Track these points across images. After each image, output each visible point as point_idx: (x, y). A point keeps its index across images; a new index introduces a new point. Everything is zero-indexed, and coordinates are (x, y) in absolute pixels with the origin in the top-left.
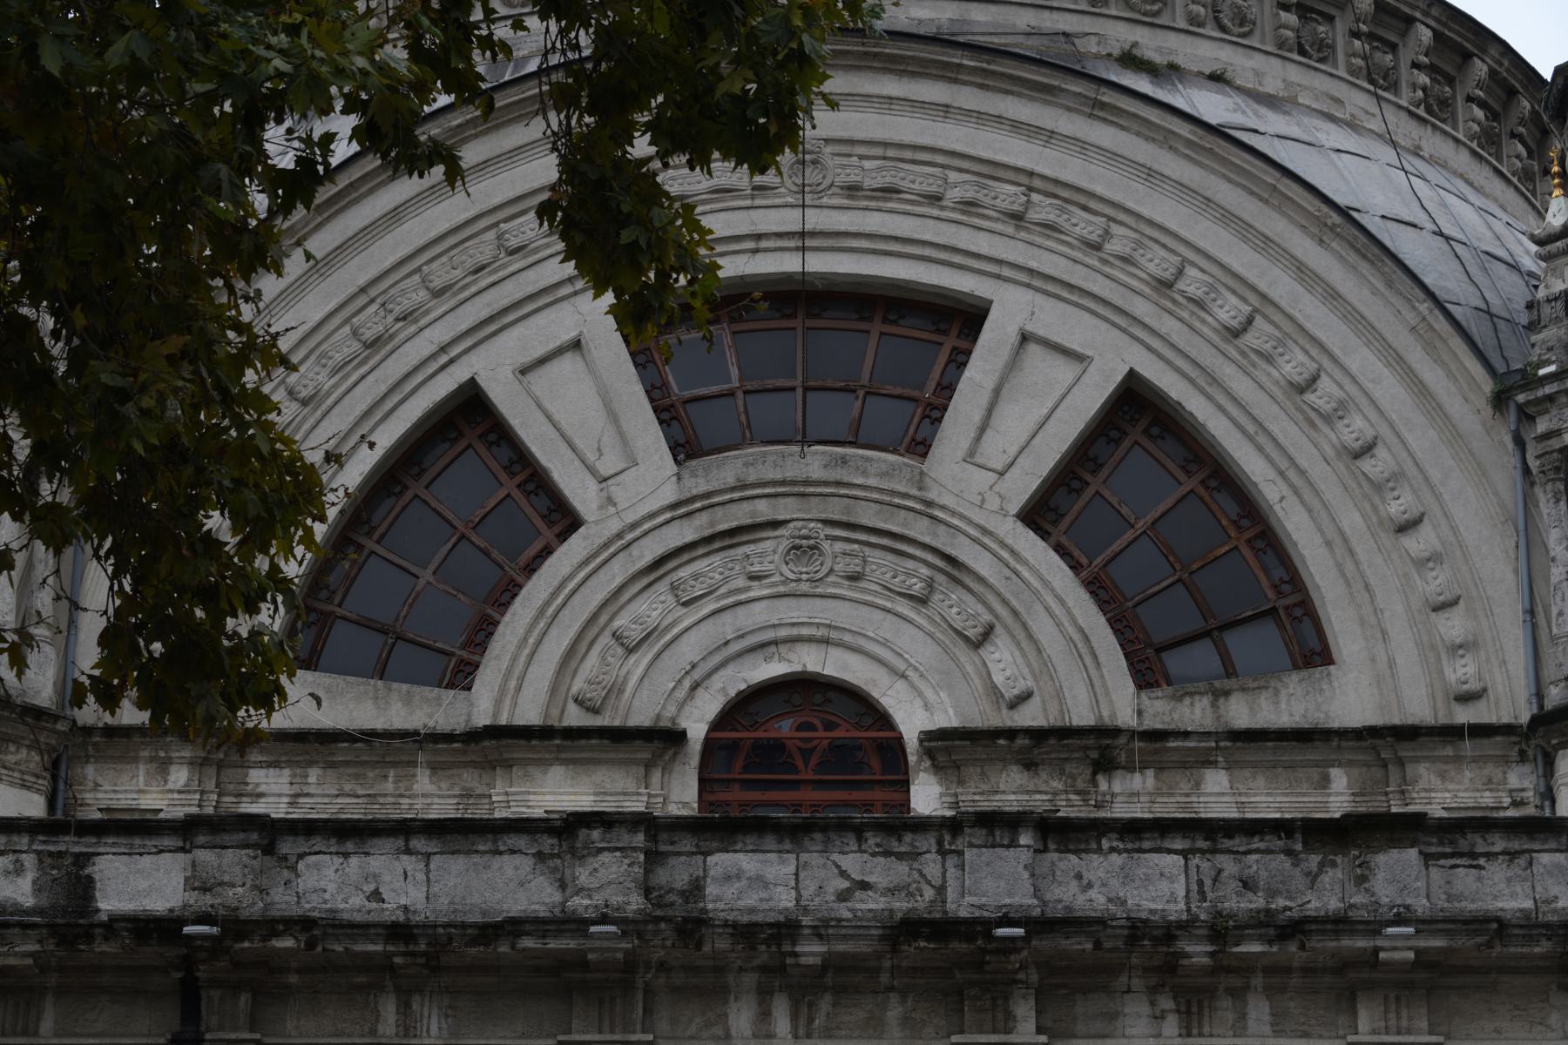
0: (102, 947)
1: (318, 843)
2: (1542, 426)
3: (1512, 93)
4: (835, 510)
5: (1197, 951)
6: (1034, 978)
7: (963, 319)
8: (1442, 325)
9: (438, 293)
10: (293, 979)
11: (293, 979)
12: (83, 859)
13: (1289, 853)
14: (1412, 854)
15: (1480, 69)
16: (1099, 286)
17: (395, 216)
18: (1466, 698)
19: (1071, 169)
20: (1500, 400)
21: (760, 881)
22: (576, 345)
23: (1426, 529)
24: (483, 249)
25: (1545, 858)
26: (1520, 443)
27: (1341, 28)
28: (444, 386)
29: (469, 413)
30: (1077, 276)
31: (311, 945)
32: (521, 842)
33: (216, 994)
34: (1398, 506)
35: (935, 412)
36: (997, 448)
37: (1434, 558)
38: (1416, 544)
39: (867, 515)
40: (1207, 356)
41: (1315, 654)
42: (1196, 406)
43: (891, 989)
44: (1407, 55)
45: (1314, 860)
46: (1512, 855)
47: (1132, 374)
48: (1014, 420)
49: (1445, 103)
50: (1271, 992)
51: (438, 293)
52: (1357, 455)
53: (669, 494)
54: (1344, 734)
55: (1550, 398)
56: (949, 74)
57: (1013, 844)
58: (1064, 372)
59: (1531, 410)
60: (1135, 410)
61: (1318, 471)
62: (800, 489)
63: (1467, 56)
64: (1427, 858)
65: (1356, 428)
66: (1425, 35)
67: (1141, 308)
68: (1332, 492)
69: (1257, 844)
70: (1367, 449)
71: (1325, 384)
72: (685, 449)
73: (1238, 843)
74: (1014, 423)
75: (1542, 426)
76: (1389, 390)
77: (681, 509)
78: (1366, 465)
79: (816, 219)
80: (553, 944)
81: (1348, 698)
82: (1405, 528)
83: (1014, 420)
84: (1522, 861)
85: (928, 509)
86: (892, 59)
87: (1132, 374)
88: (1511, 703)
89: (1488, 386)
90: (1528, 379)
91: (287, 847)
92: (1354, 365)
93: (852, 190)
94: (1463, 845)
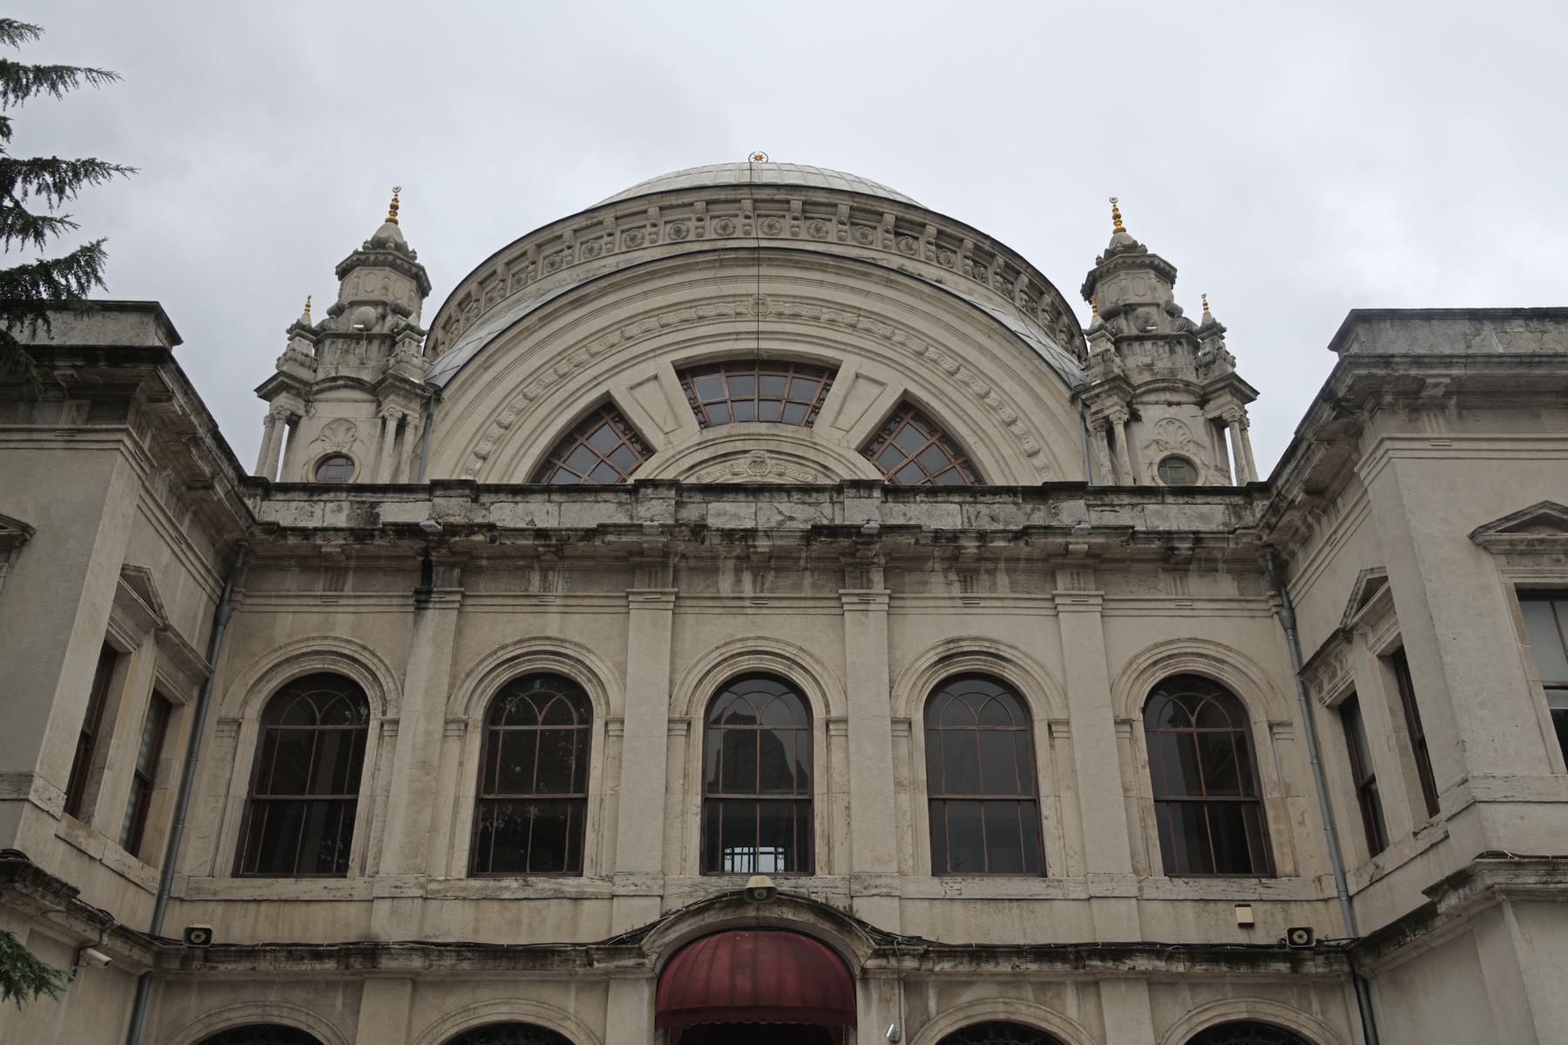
0: (378, 542)
1: (502, 497)
2: (1094, 408)
3: (1060, 314)
4: (773, 446)
5: (970, 546)
6: (883, 561)
7: (826, 371)
8: (1045, 369)
9: (593, 355)
10: (484, 563)
11: (484, 563)
12: (374, 505)
13: (1015, 504)
14: (1082, 502)
15: (1048, 299)
16: (890, 354)
17: (575, 323)
19: (877, 307)
20: (1074, 399)
21: (736, 516)
22: (656, 377)
23: (1041, 455)
24: (615, 337)
25: (1151, 507)
26: (1083, 418)
27: (990, 271)
28: (595, 394)
29: (606, 410)
30: (881, 350)
31: (493, 540)
32: (610, 496)
33: (441, 569)
34: (1029, 446)
35: (816, 410)
36: (844, 422)
37: (1046, 468)
39: (787, 448)
40: (940, 383)
42: (935, 404)
43: (806, 569)
44: (1018, 286)
45: (1029, 507)
46: (1133, 506)
47: (906, 392)
48: (851, 412)
49: (1033, 310)
50: (1008, 571)
51: (593, 355)
52: (1009, 425)
53: (697, 439)
55: (1097, 396)
56: (823, 268)
57: (870, 497)
58: (876, 390)
60: (907, 409)
61: (991, 430)
62: (757, 437)
63: (1042, 293)
64: (1088, 506)
65: (1008, 413)
66: (1026, 280)
67: (909, 363)
68: (998, 440)
69: (998, 499)
70: (1014, 422)
71: (993, 394)
72: (705, 424)
73: (988, 498)
74: (853, 410)
75: (1094, 408)
76: (1022, 397)
77: (702, 445)
78: (1013, 428)
79: (763, 327)
80: (624, 539)
82: (1031, 455)
84: (1139, 508)
85: (814, 446)
86: (797, 262)
87: (906, 392)
89: (1067, 394)
90: (1087, 389)
91: (485, 498)
92: (1006, 387)
93: (780, 315)
94: (1107, 501)
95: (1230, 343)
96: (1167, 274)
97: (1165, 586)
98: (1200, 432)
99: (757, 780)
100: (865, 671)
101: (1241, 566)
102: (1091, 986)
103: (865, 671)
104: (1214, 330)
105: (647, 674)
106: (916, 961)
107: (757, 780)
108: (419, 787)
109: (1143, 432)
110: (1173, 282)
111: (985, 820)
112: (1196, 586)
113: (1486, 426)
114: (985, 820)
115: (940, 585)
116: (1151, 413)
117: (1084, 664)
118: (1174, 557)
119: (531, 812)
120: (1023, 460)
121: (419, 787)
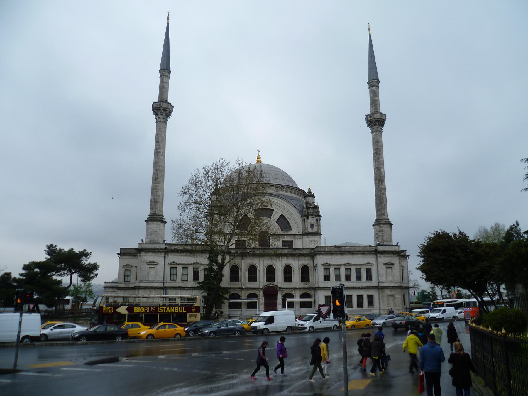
41: (291, 230)
48: (276, 216)
60: (282, 215)
76: (295, 215)
81: (292, 232)
83: (276, 216)
88: (301, 233)
95: (320, 209)
97: (304, 258)
98: (315, 221)
99: (270, 272)
100: (279, 265)
101: (310, 256)
102: (295, 290)
103: (279, 265)
104: (318, 208)
105: (261, 265)
106: (282, 289)
107: (270, 272)
108: (244, 274)
111: (288, 277)
112: (307, 258)
113: (324, 256)
114: (288, 277)
115: (285, 258)
116: (310, 218)
117: (296, 264)
118: (305, 255)
119: (253, 277)
121: (244, 274)
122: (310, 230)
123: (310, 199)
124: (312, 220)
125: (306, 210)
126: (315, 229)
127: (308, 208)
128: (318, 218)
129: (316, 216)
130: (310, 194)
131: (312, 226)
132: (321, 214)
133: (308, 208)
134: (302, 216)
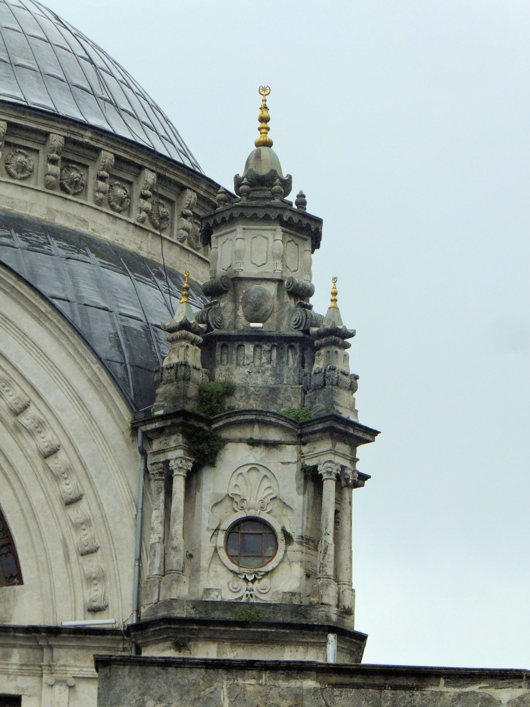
18: (94, 610)
20: (134, 429)
23: (83, 503)
34: (69, 488)
37: (87, 523)
38: (76, 513)
52: (46, 456)
54: (17, 629)
59: (150, 436)
65: (47, 439)
68: (28, 478)
70: (53, 452)
71: (32, 411)
76: (71, 417)
78: (52, 462)
82: (69, 503)
92: (50, 400)
95: (357, 358)
96: (306, 230)
104: (338, 337)
109: (216, 482)
110: (316, 244)
120: (58, 506)
122: (220, 582)
123: (251, 251)
124: (251, 476)
125: (193, 356)
126: (284, 580)
127: (214, 342)
128: (324, 455)
129: (302, 431)
130: (266, 198)
131: (250, 537)
132: (365, 409)
133: (214, 342)
134: (144, 429)
